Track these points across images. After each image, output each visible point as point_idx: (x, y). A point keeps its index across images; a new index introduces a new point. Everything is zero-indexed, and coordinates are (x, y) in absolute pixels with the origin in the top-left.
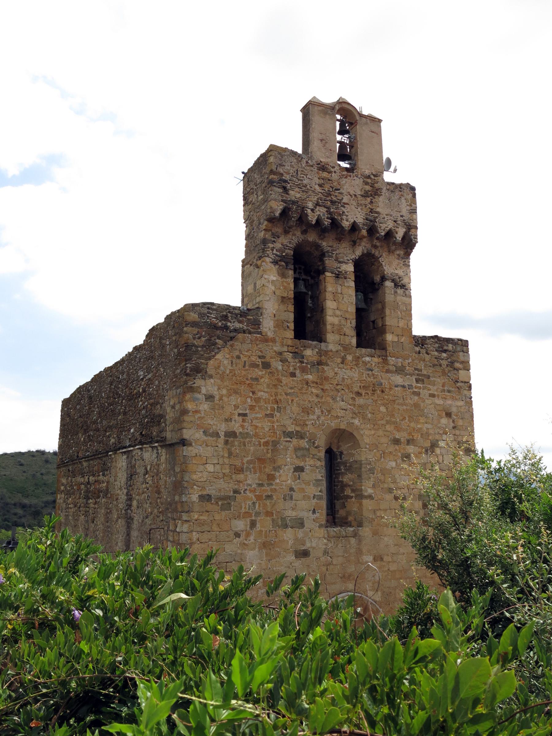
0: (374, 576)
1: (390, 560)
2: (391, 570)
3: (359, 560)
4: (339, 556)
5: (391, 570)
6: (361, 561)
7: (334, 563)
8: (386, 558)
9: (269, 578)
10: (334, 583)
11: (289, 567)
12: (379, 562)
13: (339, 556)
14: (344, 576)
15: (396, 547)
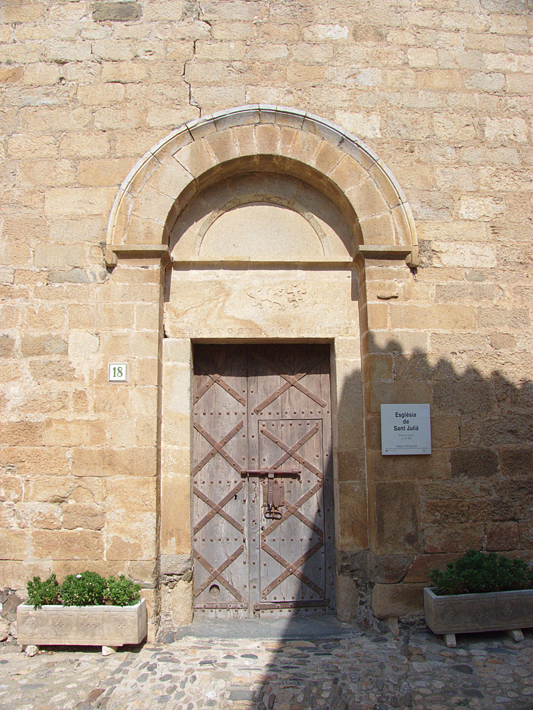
0: (354, 76)
1: (411, 40)
2: (412, 64)
3: (301, 34)
4: (233, 21)
5: (412, 64)
6: (308, 36)
7: (218, 34)
8: (393, 36)
9: (9, 63)
10: (217, 84)
11: (73, 41)
12: (370, 43)
13: (233, 21)
14: (250, 68)
15: (428, 12)
